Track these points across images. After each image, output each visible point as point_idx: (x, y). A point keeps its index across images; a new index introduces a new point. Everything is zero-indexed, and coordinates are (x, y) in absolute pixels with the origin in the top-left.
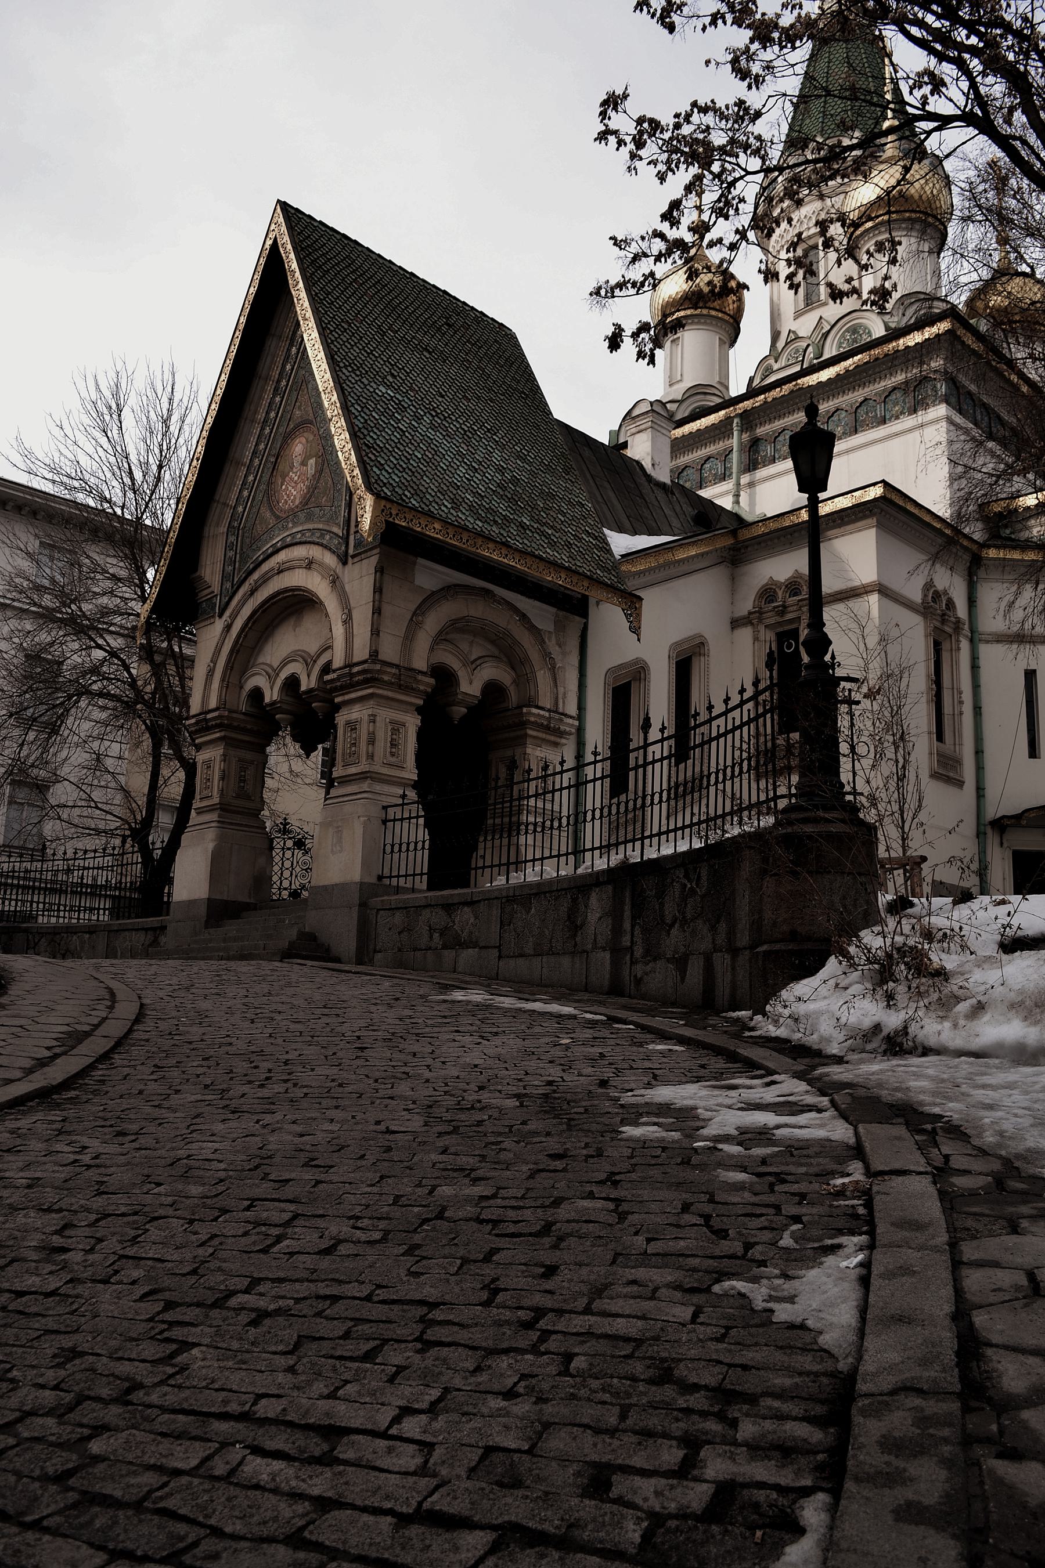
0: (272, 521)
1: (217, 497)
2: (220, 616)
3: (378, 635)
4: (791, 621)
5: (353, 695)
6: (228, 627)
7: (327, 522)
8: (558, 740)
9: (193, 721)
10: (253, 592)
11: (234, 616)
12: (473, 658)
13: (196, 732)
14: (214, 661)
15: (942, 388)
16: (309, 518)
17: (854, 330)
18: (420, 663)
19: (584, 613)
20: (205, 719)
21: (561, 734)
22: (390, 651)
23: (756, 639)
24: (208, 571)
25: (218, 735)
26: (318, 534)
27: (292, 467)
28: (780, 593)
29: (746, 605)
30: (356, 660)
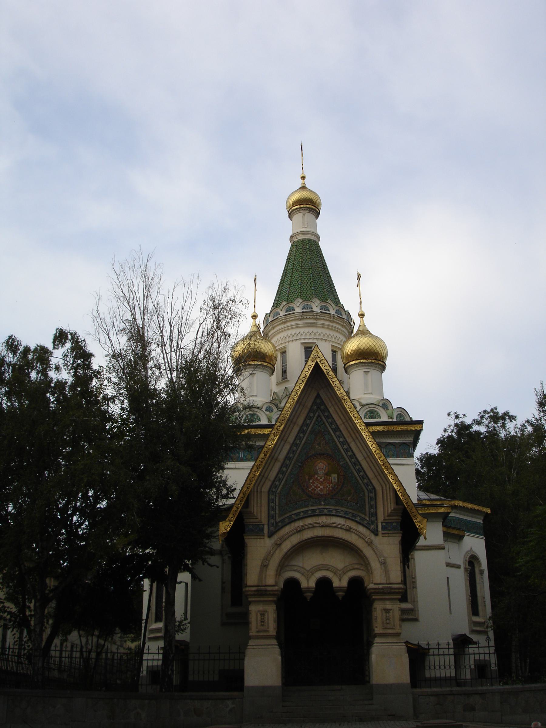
2: (270, 536)
6: (278, 545)
11: (283, 539)
13: (251, 595)
20: (266, 591)
27: (317, 474)
30: (392, 582)
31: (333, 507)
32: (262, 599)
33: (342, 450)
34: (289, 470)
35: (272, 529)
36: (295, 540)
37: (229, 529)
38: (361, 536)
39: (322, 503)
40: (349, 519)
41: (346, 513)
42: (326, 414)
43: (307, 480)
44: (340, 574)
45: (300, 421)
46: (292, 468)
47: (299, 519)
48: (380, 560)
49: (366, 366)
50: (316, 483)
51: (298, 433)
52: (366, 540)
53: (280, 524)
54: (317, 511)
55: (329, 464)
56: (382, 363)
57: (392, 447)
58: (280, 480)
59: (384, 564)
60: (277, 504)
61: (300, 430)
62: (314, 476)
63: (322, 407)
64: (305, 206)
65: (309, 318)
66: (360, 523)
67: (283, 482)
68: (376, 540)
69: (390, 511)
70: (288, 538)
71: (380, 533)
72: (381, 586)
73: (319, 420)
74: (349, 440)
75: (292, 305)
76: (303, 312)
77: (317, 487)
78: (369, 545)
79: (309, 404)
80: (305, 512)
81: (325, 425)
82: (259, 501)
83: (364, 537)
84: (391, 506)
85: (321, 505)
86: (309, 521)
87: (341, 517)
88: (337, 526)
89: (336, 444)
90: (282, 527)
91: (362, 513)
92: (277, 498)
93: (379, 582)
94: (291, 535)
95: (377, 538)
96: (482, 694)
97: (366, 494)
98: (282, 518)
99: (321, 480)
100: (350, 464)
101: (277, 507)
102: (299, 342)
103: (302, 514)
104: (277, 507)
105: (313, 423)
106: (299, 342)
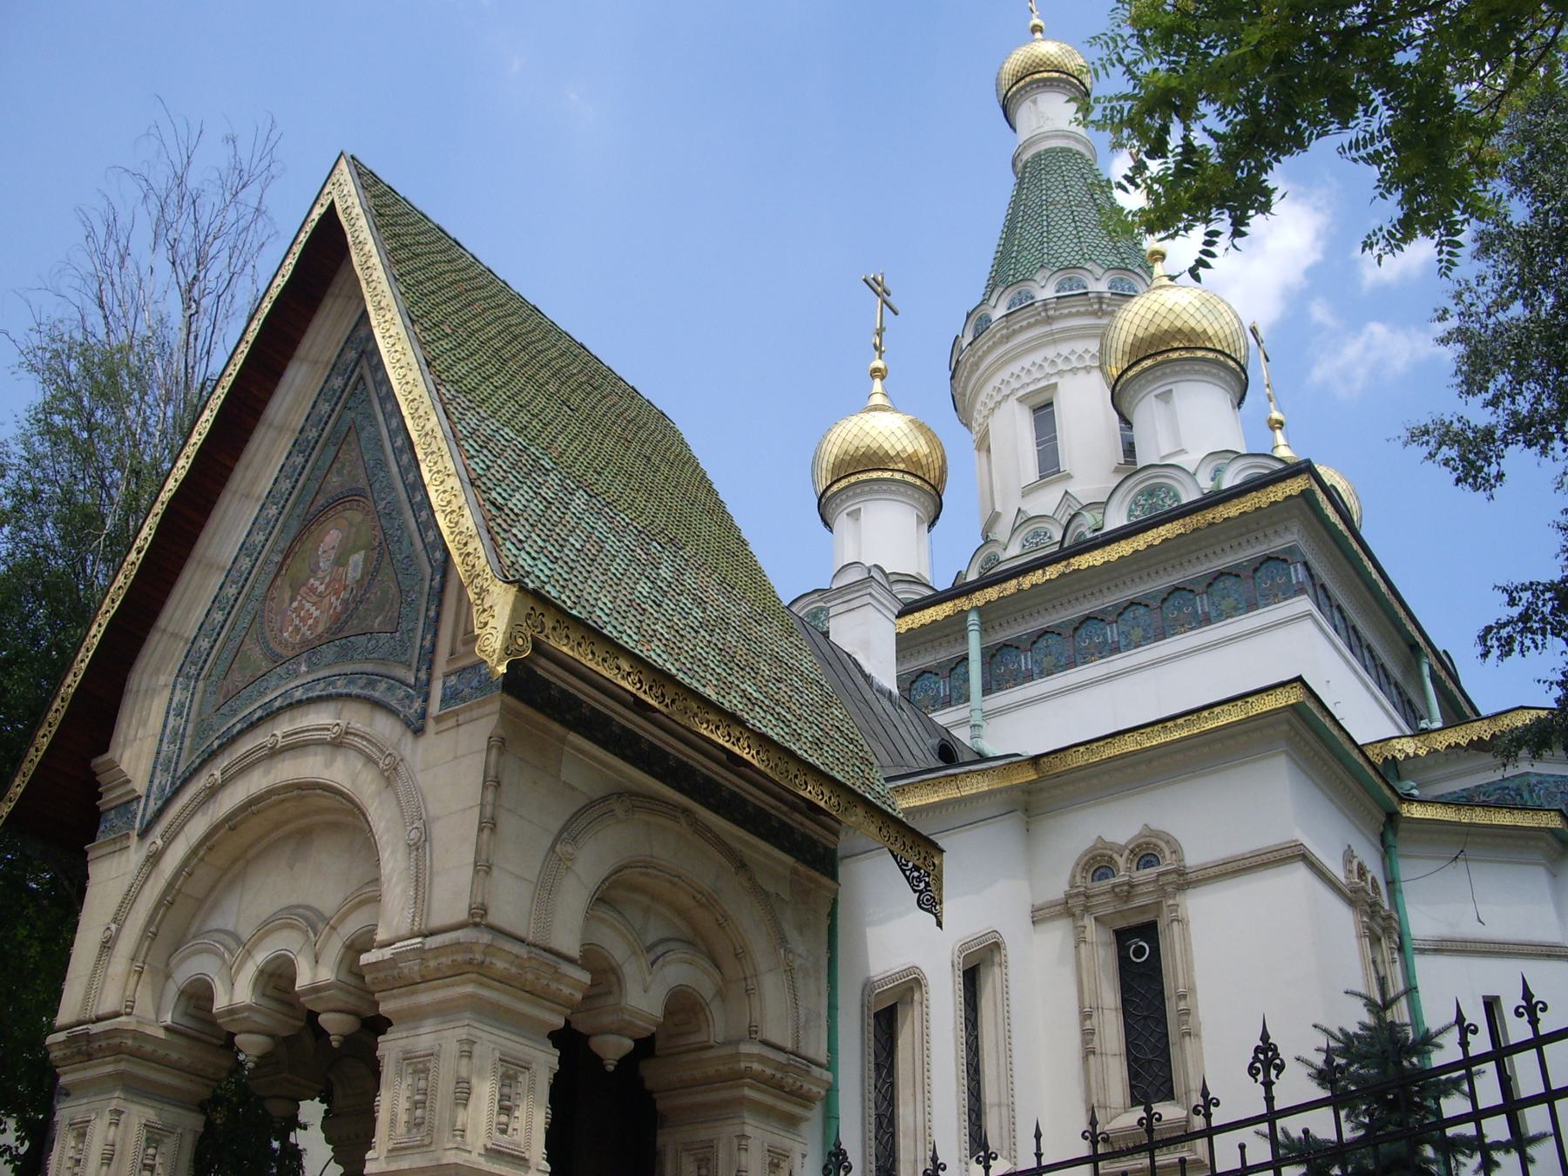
0: (265, 665)
1: (162, 622)
2: (143, 834)
3: (489, 869)
4: (1143, 909)
6: (154, 859)
7: (383, 660)
8: (797, 1110)
9: (61, 1036)
10: (213, 792)
11: (170, 838)
12: (651, 938)
14: (119, 918)
15: (1298, 574)
16: (344, 655)
17: (1151, 492)
18: (568, 941)
19: (833, 875)
21: (805, 1099)
22: (511, 909)
23: (1080, 941)
24: (127, 755)
25: (109, 1069)
26: (362, 682)
28: (1121, 862)
29: (1057, 887)
30: (436, 921)
32: (90, 1073)
36: (197, 829)
41: (350, 677)
46: (256, 580)
49: (1157, 379)
50: (308, 605)
57: (1229, 582)
60: (192, 716)
65: (1029, 326)
71: (431, 724)
72: (387, 953)
73: (360, 387)
83: (376, 754)
94: (193, 814)
99: (321, 588)
100: (403, 496)
102: (1013, 399)
104: (190, 727)
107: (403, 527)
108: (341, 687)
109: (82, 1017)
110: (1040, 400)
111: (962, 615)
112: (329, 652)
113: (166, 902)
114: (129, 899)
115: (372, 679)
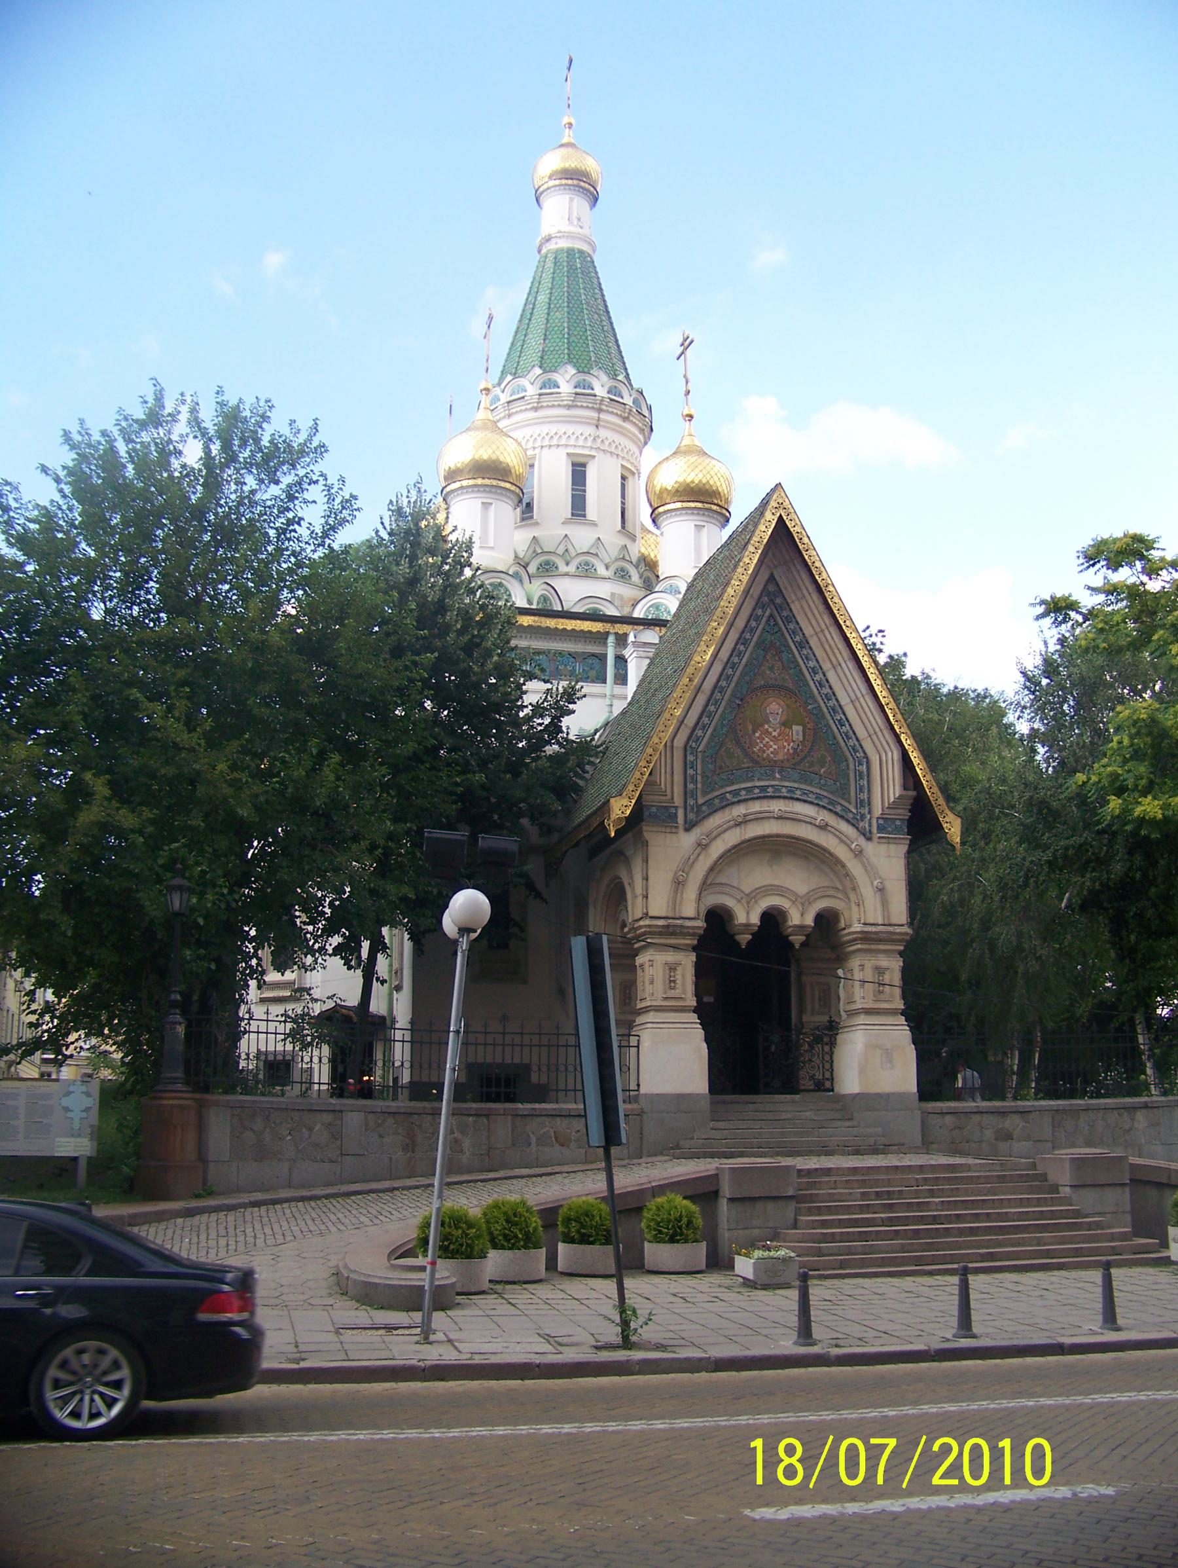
0: (746, 764)
2: (687, 830)
5: (881, 947)
6: (702, 846)
7: (832, 793)
11: (713, 837)
16: (804, 779)
27: (768, 722)
31: (796, 785)
33: (811, 683)
34: (720, 711)
35: (691, 816)
37: (628, 812)
38: (843, 840)
39: (777, 776)
40: (824, 807)
41: (818, 797)
42: (785, 613)
43: (750, 732)
44: (804, 901)
45: (740, 623)
47: (739, 802)
48: (875, 883)
51: (736, 644)
52: (853, 846)
53: (704, 808)
54: (770, 790)
55: (788, 706)
56: (724, 511)
58: (704, 728)
59: (881, 890)
61: (739, 638)
62: (762, 725)
63: (778, 601)
64: (575, 182)
66: (842, 817)
67: (710, 731)
68: (870, 848)
69: (892, 800)
70: (719, 835)
71: (875, 839)
72: (873, 929)
74: (826, 666)
75: (556, 377)
76: (577, 394)
77: (767, 746)
78: (856, 856)
79: (756, 591)
80: (749, 790)
81: (783, 635)
82: (669, 761)
84: (895, 790)
85: (774, 779)
86: (756, 807)
87: (811, 803)
88: (802, 818)
89: (801, 671)
90: (710, 815)
91: (845, 800)
92: (699, 761)
93: (872, 921)
94: (725, 831)
95: (869, 843)
96: (1022, 1113)
97: (852, 766)
98: (706, 798)
99: (774, 734)
100: (825, 710)
101: (699, 778)
103: (743, 793)
104: (699, 778)
105: (761, 627)
106: (562, 453)
107: (827, 725)
108: (812, 798)
109: (671, 915)
110: (581, 460)
111: (607, 633)
112: (796, 776)
113: (712, 869)
114: (688, 865)
115: (831, 802)
